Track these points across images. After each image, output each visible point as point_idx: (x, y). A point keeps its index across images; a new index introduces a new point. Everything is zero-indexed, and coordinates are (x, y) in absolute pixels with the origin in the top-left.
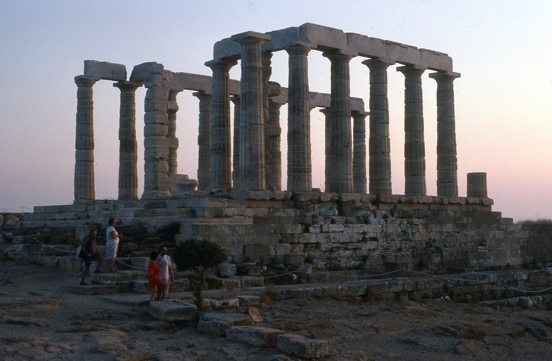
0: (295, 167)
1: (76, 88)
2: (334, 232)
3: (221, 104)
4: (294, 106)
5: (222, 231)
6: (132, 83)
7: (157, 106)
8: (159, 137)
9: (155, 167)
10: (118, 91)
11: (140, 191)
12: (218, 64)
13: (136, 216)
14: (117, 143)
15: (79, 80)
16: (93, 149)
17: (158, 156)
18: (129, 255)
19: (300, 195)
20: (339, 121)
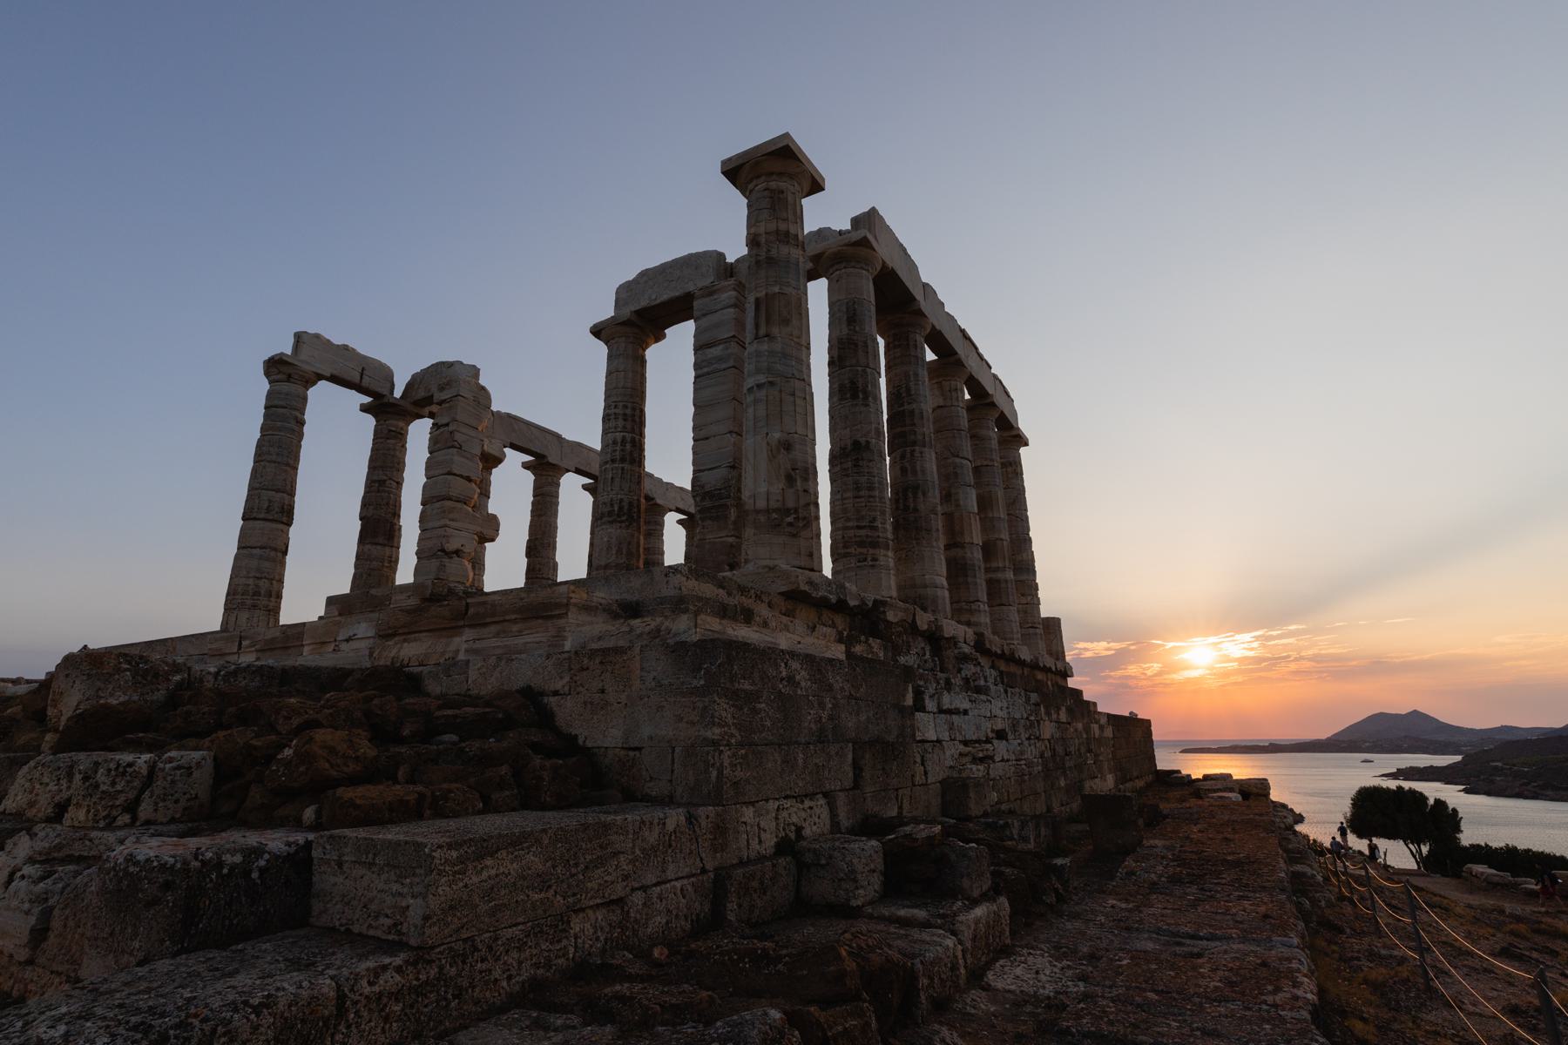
0: (863, 532)
1: (265, 386)
2: (956, 712)
3: (628, 411)
4: (853, 383)
5: (790, 679)
6: (402, 403)
7: (457, 436)
8: (459, 505)
9: (442, 567)
10: (370, 422)
11: (405, 574)
12: (623, 324)
13: (386, 634)
14: (353, 527)
15: (276, 367)
16: (289, 524)
17: (452, 546)
18: (309, 814)
19: (884, 603)
20: (917, 454)
